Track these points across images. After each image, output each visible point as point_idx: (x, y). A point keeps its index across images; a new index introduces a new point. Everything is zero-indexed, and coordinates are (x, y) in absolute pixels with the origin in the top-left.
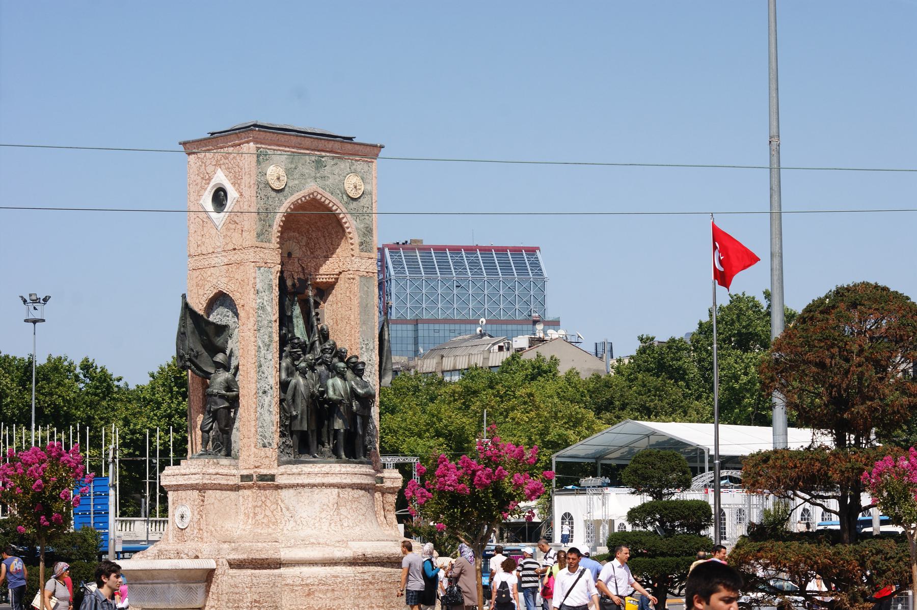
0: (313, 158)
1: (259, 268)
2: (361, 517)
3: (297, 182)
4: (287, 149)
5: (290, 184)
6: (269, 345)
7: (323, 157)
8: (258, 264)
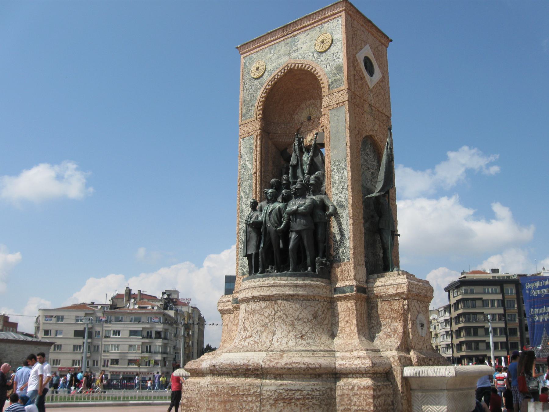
0: (288, 41)
1: (243, 139)
2: (258, 328)
3: (274, 65)
4: (266, 46)
5: (269, 68)
6: (249, 194)
7: (295, 36)
8: (242, 137)
